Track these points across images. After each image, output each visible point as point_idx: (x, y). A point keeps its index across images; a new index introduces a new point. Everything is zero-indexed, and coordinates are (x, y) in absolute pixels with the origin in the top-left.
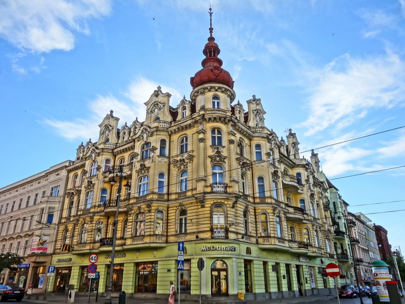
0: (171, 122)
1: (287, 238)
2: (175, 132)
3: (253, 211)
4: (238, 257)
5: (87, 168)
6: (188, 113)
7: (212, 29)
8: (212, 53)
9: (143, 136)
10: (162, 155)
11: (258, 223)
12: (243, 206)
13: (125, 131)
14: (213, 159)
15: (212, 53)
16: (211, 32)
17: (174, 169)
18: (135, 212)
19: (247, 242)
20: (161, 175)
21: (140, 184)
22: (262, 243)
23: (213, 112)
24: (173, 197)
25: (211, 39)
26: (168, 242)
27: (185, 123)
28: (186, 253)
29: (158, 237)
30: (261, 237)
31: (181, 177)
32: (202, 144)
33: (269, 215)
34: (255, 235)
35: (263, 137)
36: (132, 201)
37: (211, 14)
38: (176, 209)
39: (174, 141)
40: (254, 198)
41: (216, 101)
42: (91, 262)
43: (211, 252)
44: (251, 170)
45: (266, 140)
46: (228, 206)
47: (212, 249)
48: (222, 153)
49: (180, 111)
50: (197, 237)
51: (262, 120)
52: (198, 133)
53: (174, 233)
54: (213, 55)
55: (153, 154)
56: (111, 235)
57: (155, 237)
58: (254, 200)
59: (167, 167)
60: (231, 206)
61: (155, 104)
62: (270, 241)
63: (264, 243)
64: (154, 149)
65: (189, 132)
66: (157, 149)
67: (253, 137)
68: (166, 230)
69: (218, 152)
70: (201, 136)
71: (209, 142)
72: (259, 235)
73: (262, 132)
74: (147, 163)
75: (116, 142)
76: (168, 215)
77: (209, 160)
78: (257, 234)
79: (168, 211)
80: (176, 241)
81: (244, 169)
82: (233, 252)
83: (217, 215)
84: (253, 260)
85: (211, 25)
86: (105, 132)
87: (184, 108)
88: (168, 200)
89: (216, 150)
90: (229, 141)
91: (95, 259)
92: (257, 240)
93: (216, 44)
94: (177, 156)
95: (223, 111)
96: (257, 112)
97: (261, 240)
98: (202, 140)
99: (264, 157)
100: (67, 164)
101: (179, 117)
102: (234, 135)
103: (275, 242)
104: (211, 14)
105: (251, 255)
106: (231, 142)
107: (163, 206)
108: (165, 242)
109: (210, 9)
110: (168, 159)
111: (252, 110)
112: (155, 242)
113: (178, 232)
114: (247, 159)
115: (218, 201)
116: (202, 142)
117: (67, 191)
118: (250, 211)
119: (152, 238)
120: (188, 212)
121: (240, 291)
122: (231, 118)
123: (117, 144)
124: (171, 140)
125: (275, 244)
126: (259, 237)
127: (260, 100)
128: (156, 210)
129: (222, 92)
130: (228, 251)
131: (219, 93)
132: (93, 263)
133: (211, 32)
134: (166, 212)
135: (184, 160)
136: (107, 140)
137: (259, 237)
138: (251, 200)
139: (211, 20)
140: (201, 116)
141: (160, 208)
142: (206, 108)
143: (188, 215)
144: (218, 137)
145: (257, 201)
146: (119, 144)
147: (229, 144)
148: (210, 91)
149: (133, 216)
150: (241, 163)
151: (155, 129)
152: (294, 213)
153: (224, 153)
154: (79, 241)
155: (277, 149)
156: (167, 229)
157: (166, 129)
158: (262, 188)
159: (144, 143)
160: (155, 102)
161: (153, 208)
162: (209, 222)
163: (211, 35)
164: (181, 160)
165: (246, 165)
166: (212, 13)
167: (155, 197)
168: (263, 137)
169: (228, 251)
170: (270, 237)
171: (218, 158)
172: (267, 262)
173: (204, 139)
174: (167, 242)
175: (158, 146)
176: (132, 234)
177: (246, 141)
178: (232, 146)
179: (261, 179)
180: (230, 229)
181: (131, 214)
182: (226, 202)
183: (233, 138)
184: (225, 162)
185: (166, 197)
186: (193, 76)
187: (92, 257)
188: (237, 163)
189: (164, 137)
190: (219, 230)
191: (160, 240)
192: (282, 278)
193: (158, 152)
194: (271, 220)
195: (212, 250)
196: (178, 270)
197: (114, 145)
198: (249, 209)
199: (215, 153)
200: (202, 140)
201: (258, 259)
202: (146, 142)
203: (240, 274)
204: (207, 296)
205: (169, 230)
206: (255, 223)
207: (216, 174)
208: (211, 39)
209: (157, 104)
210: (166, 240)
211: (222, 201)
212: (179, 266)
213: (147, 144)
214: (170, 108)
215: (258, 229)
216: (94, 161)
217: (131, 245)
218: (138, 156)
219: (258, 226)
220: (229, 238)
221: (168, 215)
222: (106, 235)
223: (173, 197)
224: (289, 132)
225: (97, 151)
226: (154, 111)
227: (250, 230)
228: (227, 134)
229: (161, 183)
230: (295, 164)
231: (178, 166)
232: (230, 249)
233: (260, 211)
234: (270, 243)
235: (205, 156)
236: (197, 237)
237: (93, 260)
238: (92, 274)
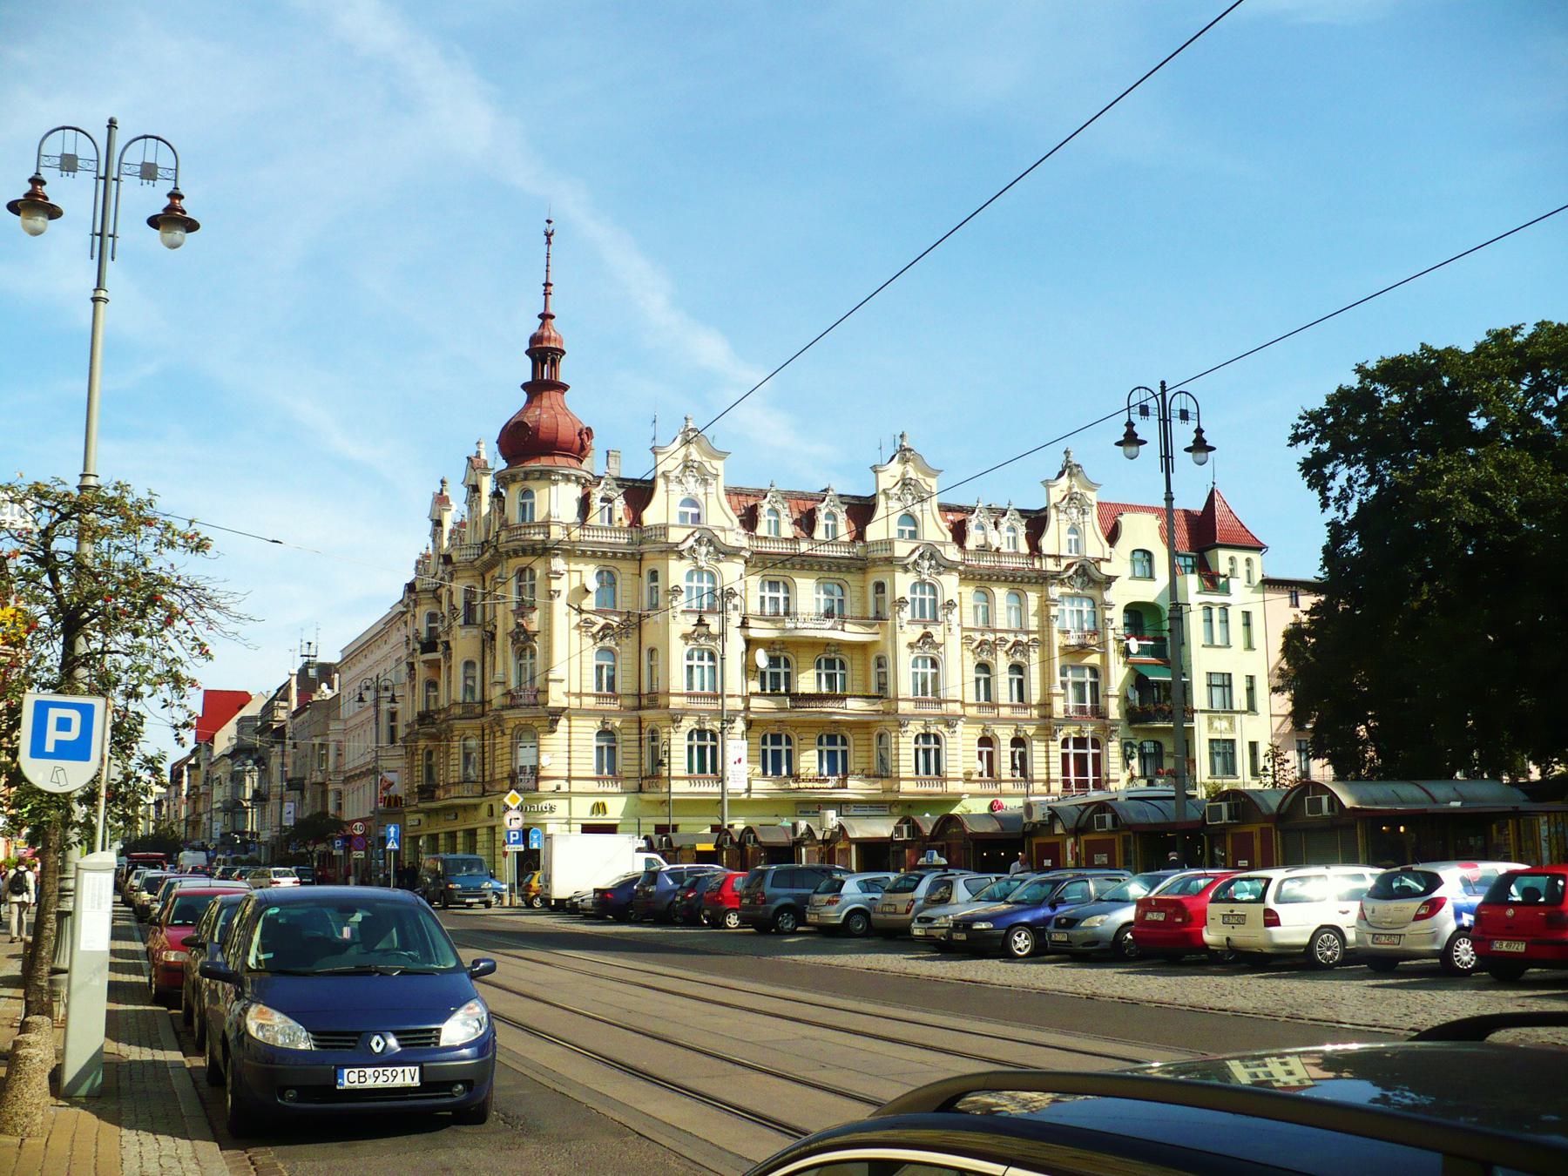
10: (469, 621)
37: (548, 235)
41: (528, 501)
88: (483, 715)
96: (686, 467)
107: (469, 727)
131: (530, 484)
167: (458, 711)
180: (543, 773)
185: (478, 710)
189: (470, 582)
193: (461, 621)
224: (899, 441)
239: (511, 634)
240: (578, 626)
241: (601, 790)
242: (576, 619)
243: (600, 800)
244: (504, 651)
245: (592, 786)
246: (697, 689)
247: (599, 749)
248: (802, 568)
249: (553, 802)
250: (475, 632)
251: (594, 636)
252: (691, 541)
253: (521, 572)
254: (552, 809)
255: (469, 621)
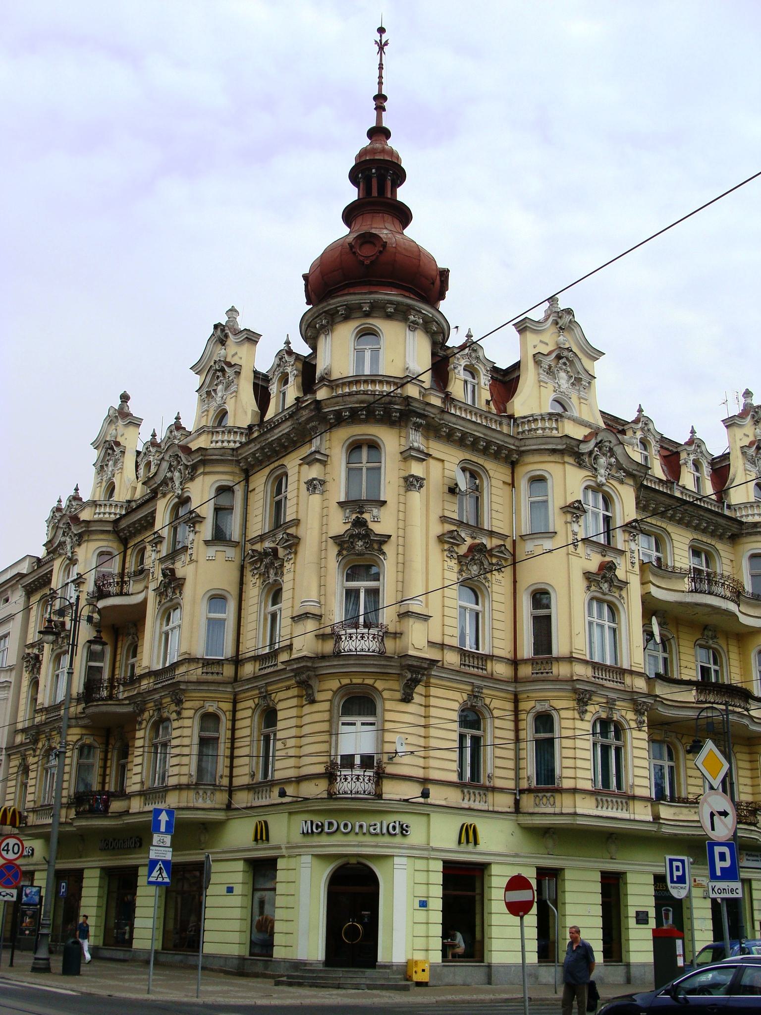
0: (250, 427)
1: (639, 792)
2: (260, 462)
3: (510, 706)
4: (425, 854)
5: (56, 582)
6: (292, 392)
7: (385, 98)
8: (374, 182)
9: (172, 479)
10: (219, 537)
11: (523, 745)
12: (461, 691)
13: (151, 458)
14: (346, 546)
15: (374, 182)
16: (380, 109)
17: (254, 581)
18: (151, 717)
19: (470, 809)
20: (217, 599)
21: (165, 628)
22: (531, 811)
23: (354, 389)
24: (248, 669)
25: (379, 133)
26: (233, 806)
27: (276, 431)
28: (267, 839)
29: (201, 792)
30: (529, 791)
31: (273, 605)
32: (316, 499)
33: (561, 719)
34: (511, 784)
35: (554, 451)
36: (145, 684)
37: (382, 46)
38: (253, 706)
39: (257, 491)
40: (515, 663)
42: (4, 858)
43: (324, 840)
44: (508, 571)
45: (570, 460)
46: (386, 694)
47: (326, 830)
48: (371, 526)
49: (274, 388)
50: (283, 794)
51: (583, 381)
52: (309, 461)
53: (246, 780)
54: (375, 193)
55: (191, 536)
56: (116, 784)
57: (192, 794)
58: (516, 670)
59: (236, 574)
60: (398, 695)
61: (216, 370)
62: (558, 804)
63: (537, 810)
64: (194, 520)
65: (292, 463)
66: (203, 524)
67: (522, 453)
68: (227, 772)
69: (360, 523)
70: (314, 472)
71: (339, 491)
72: (524, 785)
73: (555, 432)
74: (182, 568)
75: (128, 498)
76: (233, 725)
77: (333, 550)
78: (517, 778)
79: (234, 711)
80: (249, 805)
81: (475, 569)
82: (398, 840)
83: (354, 724)
84: (489, 864)
85: (380, 83)
86: (107, 465)
87: (284, 380)
89: (354, 516)
90: (406, 479)
91: (16, 851)
92: (517, 803)
93: (392, 152)
94: (262, 538)
95: (388, 383)
96: (559, 357)
97: (527, 802)
98: (313, 485)
99: (557, 521)
100: (24, 569)
101: (270, 414)
102: (424, 457)
103: (575, 807)
104: (382, 46)
105: (481, 847)
106: (412, 483)
108: (225, 807)
109: (381, 30)
110: (238, 549)
111: (534, 356)
112: (191, 805)
113: (259, 777)
114: (491, 534)
115: (355, 681)
116: (314, 492)
117: (27, 651)
118: (491, 707)
119: (184, 794)
120: (280, 715)
121: (419, 956)
122: (409, 405)
123: (129, 502)
124: (250, 489)
125: (575, 814)
126: (522, 792)
127: (569, 311)
128: (196, 711)
129: (389, 317)
130: (376, 834)
132: (10, 861)
133: (380, 109)
134: (229, 715)
135: (275, 551)
136: (111, 489)
137: (522, 792)
138: (502, 670)
139: (381, 67)
140: (312, 407)
141: (211, 708)
142: (334, 377)
143: (280, 725)
144: (368, 469)
145: (525, 671)
146: (135, 501)
147: (402, 490)
148: (347, 318)
149: (145, 728)
150: (463, 550)
151: (197, 458)
152: (698, 702)
153: (383, 523)
154: (39, 797)
155: (622, 482)
156: (231, 767)
157: (230, 452)
158: (543, 627)
159: (176, 500)
160: (215, 363)
161: (187, 705)
162: (324, 747)
163: (379, 118)
164: (266, 554)
165: (479, 557)
166: (386, 44)
167: (196, 673)
168: (554, 451)
169: (376, 834)
170: (560, 791)
171: (360, 543)
172: (562, 869)
173: (323, 483)
174: (229, 807)
175: (207, 512)
176: (142, 783)
177: (497, 472)
178: (416, 498)
179: (541, 597)
180: (390, 769)
181: (140, 723)
182: (379, 685)
183: (417, 469)
184: (384, 553)
186: (307, 271)
187: (8, 844)
188: (443, 550)
189: (226, 480)
190: (358, 773)
191: (209, 802)
192: (632, 922)
193: (206, 530)
194: (565, 733)
195: (328, 834)
196: (255, 890)
197: (122, 506)
198: (487, 701)
199: (348, 526)
200: (313, 485)
201: (512, 859)
202: (179, 497)
203: (423, 904)
204: (311, 964)
205: (236, 772)
206: (512, 746)
207: (357, 591)
208: (379, 133)
209: (222, 370)
210: (226, 802)
211: (367, 681)
212: (155, 873)
213: (184, 501)
214: (255, 377)
215: (523, 764)
216: (70, 559)
217: (139, 813)
218: (161, 542)
219: (523, 754)
220: (385, 796)
221: (233, 725)
222: (103, 783)
223: (248, 669)
224: (742, 400)
225: (75, 530)
226: (215, 390)
227: (489, 770)
228: (399, 457)
229: (215, 625)
230: (741, 523)
231: (263, 569)
232: (385, 831)
233: (532, 704)
234: (557, 810)
235: (324, 539)
236: (283, 794)
237: (11, 852)
238: (8, 891)
239: (338, 540)
240: (441, 539)
241: (465, 804)
242: (437, 529)
243: (469, 821)
244: (321, 568)
245: (453, 797)
246: (596, 659)
247: (462, 737)
248: (680, 522)
249: (405, 819)
250: (231, 552)
251: (460, 559)
252: (591, 445)
253: (355, 447)
254: (404, 831)
255: (219, 537)
